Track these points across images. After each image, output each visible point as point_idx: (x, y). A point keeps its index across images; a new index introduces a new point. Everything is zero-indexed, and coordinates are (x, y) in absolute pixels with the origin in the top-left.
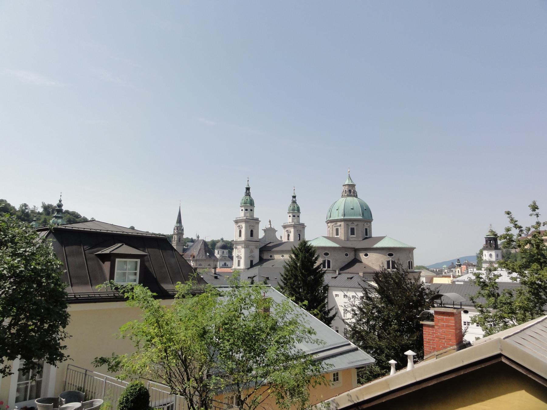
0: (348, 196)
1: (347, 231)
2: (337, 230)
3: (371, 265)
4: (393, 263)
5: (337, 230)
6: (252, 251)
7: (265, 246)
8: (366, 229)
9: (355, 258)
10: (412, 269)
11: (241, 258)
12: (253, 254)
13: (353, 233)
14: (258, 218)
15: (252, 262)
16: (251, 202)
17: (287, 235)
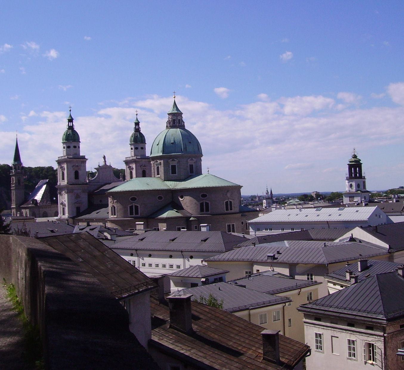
0: (172, 127)
6: (78, 196)
10: (231, 209)
13: (174, 171)
14: (85, 156)
15: (78, 209)
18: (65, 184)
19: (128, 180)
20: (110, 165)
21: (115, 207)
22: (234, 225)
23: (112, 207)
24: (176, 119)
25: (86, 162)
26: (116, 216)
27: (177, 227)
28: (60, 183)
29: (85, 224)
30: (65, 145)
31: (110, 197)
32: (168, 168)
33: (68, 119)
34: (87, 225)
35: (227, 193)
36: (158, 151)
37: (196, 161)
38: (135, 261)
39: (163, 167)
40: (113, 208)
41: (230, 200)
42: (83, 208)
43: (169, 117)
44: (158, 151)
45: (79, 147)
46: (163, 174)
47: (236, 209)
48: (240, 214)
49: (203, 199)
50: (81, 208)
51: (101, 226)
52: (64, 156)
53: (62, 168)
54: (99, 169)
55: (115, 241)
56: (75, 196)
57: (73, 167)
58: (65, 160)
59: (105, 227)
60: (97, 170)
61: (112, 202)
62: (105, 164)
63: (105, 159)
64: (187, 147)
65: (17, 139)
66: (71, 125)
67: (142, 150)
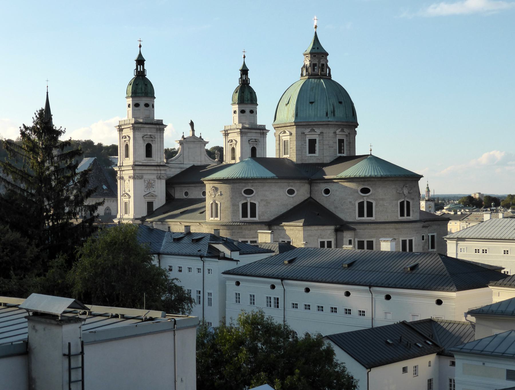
6: (150, 185)
9: (310, 197)
10: (408, 215)
12: (153, 190)
14: (162, 120)
15: (150, 205)
20: (201, 137)
21: (217, 205)
24: (317, 63)
26: (218, 219)
32: (303, 143)
35: (403, 187)
37: (349, 133)
38: (278, 299)
40: (214, 205)
45: (153, 107)
46: (294, 152)
49: (364, 196)
54: (184, 142)
55: (239, 261)
57: (143, 137)
62: (193, 135)
64: (336, 110)
65: (47, 93)
66: (140, 69)
67: (252, 115)
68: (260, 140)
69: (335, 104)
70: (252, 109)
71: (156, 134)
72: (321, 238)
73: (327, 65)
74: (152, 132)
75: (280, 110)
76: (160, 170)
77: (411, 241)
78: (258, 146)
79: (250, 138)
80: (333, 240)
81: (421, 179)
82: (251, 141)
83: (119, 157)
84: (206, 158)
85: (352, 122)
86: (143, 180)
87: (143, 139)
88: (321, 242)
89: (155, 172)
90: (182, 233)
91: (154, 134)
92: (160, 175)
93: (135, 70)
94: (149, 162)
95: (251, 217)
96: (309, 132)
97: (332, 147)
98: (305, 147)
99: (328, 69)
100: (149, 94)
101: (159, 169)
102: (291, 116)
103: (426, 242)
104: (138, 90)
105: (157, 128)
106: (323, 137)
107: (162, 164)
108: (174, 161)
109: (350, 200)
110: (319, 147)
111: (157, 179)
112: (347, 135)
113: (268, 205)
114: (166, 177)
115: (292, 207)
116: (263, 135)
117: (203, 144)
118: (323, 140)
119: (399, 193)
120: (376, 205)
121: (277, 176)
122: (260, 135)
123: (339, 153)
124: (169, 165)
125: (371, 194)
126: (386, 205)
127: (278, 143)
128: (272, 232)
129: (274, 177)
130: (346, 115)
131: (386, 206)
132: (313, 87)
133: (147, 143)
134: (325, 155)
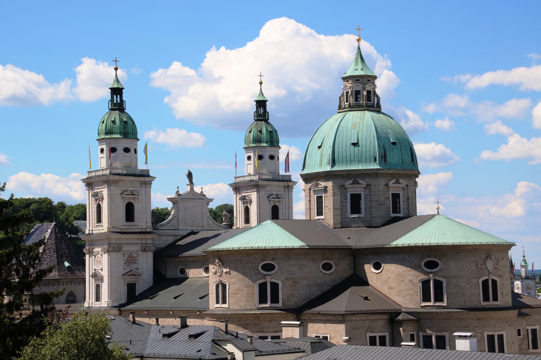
0: (352, 108)
1: (341, 202)
2: (319, 200)
3: (387, 291)
4: (438, 285)
5: (319, 200)
6: (131, 260)
7: (173, 245)
8: (396, 197)
9: (354, 275)
10: (495, 299)
11: (102, 280)
13: (356, 208)
14: (148, 171)
15: (131, 287)
16: (125, 128)
17: (243, 208)
18: (104, 231)
19: (238, 226)
20: (202, 192)
21: (224, 286)
22: (502, 335)
23: (217, 286)
24: (361, 89)
25: (152, 184)
26: (226, 306)
27: (369, 334)
28: (91, 229)
29: (177, 322)
30: (105, 146)
31: (213, 263)
32: (343, 200)
33: (111, 87)
34: (180, 326)
36: (321, 161)
37: (407, 186)
39: (332, 198)
41: (494, 278)
42: (142, 285)
43: (346, 86)
44: (321, 161)
45: (136, 152)
47: (504, 300)
48: (516, 312)
50: (137, 286)
51: (216, 329)
52: (103, 170)
53: (97, 195)
56: (125, 258)
57: (121, 194)
58: (105, 178)
59: (227, 332)
60: (174, 203)
61: (218, 274)
62: (192, 189)
63: (192, 178)
64: (388, 153)
66: (117, 101)
67: (272, 161)
68: (284, 196)
69: (387, 145)
70: (272, 153)
71: (140, 189)
72: (372, 332)
73: (375, 92)
74: (134, 187)
75: (310, 155)
76: (146, 239)
77: (501, 337)
78: (281, 204)
79: (270, 193)
80: (387, 334)
81: (513, 248)
82: (271, 197)
83: (88, 221)
84: (210, 221)
85: (411, 170)
86: (122, 253)
87: (121, 196)
88: (370, 337)
89: (139, 242)
90: (174, 327)
91: (137, 189)
92: (145, 245)
93: (110, 102)
94: (130, 227)
95: (272, 302)
96: (351, 184)
97: (384, 205)
98: (345, 204)
99: (376, 98)
100: (130, 135)
101: (144, 237)
102: (326, 162)
103: (524, 339)
104: (114, 129)
105: (142, 181)
106: (370, 191)
107: (148, 230)
108: (165, 226)
109: (411, 278)
110: (365, 204)
111: (142, 251)
112: (403, 188)
113: (295, 286)
114: (153, 248)
115: (329, 288)
116: (288, 188)
117: (206, 202)
118: (370, 194)
119: (481, 269)
120: (448, 285)
121: (308, 246)
122: (283, 189)
123: (393, 213)
124: (158, 232)
125: (440, 270)
126: (462, 284)
127: (309, 199)
128: (302, 324)
129: (303, 246)
130: (402, 160)
131: (462, 286)
132: (356, 123)
133: (127, 202)
134: (373, 215)
